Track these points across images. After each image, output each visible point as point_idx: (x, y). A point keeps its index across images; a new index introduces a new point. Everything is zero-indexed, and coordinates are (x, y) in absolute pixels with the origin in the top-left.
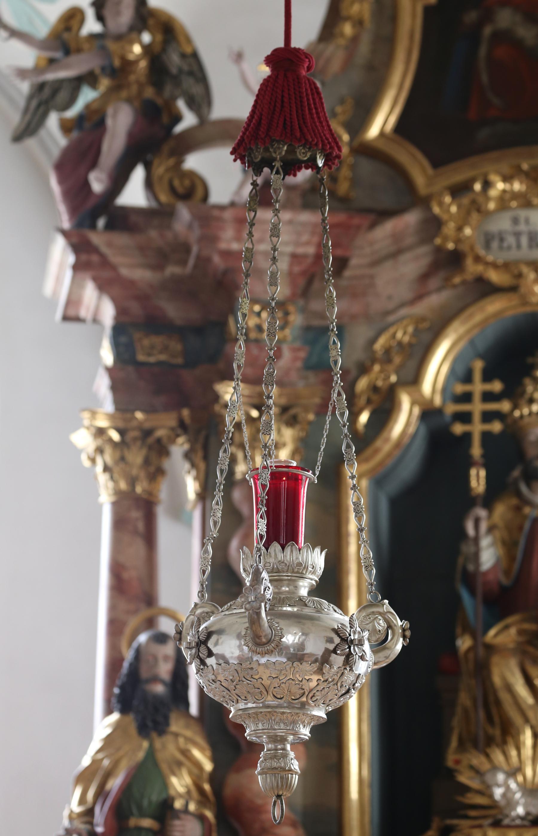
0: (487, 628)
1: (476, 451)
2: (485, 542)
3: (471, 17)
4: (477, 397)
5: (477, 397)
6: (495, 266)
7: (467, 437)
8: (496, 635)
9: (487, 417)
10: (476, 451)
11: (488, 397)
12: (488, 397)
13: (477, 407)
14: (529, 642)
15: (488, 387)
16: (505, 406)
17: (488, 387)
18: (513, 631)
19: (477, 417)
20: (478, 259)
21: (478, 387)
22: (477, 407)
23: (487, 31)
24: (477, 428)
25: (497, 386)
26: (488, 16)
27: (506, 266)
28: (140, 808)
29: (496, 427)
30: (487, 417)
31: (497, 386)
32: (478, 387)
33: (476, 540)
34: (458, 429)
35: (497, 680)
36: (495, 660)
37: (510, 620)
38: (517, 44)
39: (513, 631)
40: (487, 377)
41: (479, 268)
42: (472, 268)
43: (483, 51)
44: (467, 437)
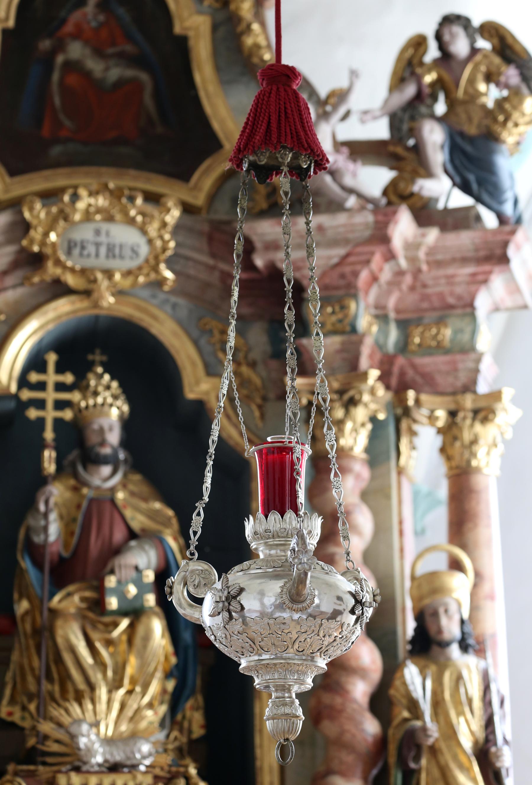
0: (52, 595)
1: (49, 435)
2: (53, 516)
3: (45, 44)
4: (50, 387)
5: (50, 387)
6: (72, 270)
7: (41, 421)
8: (60, 601)
9: (60, 405)
10: (49, 435)
11: (60, 387)
12: (60, 387)
13: (51, 396)
14: (89, 609)
15: (61, 378)
16: (75, 396)
17: (61, 378)
18: (76, 598)
19: (50, 405)
20: (58, 262)
22: (51, 396)
23: (60, 59)
24: (50, 414)
26: (60, 47)
27: (83, 272)
29: (68, 415)
30: (60, 405)
32: (51, 377)
33: (46, 516)
34: (33, 413)
35: (60, 641)
36: (59, 623)
37: (71, 588)
38: (87, 75)
39: (76, 598)
40: (60, 369)
41: (58, 271)
42: (52, 270)
43: (56, 77)
44: (41, 421)
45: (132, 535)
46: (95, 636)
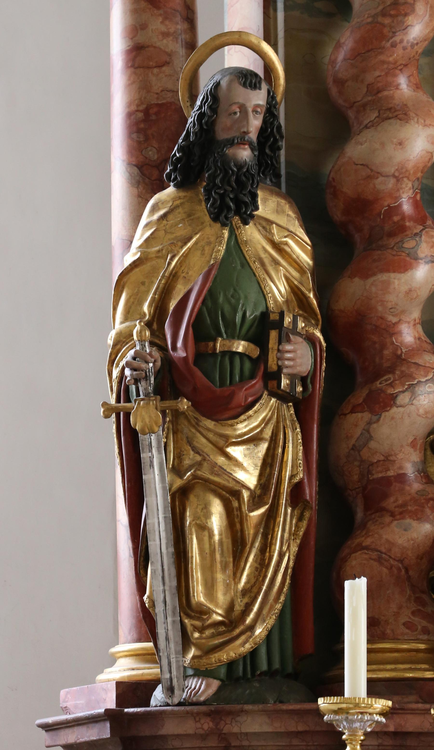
28: (230, 325)
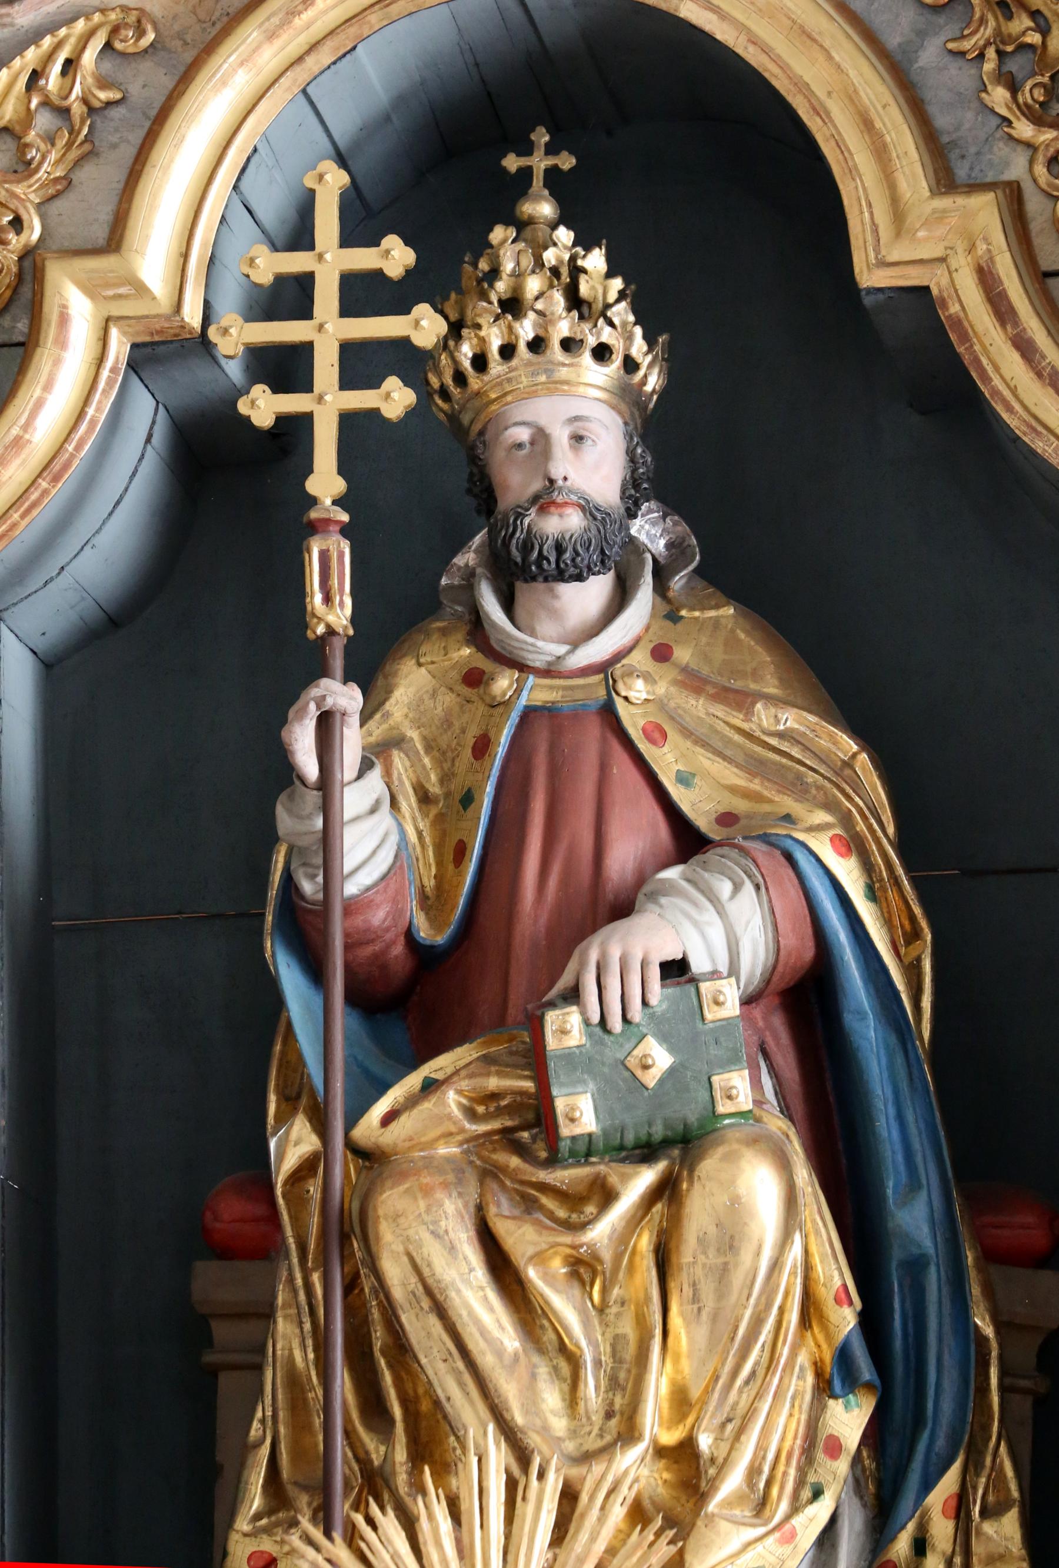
1: (325, 482)
9: (361, 364)
10: (325, 482)
11: (363, 294)
12: (363, 294)
13: (327, 331)
15: (363, 259)
16: (424, 326)
17: (363, 259)
21: (330, 261)
22: (327, 331)
24: (327, 402)
25: (395, 257)
29: (394, 398)
31: (395, 257)
32: (330, 261)
45: (688, 842)
46: (520, 1238)
